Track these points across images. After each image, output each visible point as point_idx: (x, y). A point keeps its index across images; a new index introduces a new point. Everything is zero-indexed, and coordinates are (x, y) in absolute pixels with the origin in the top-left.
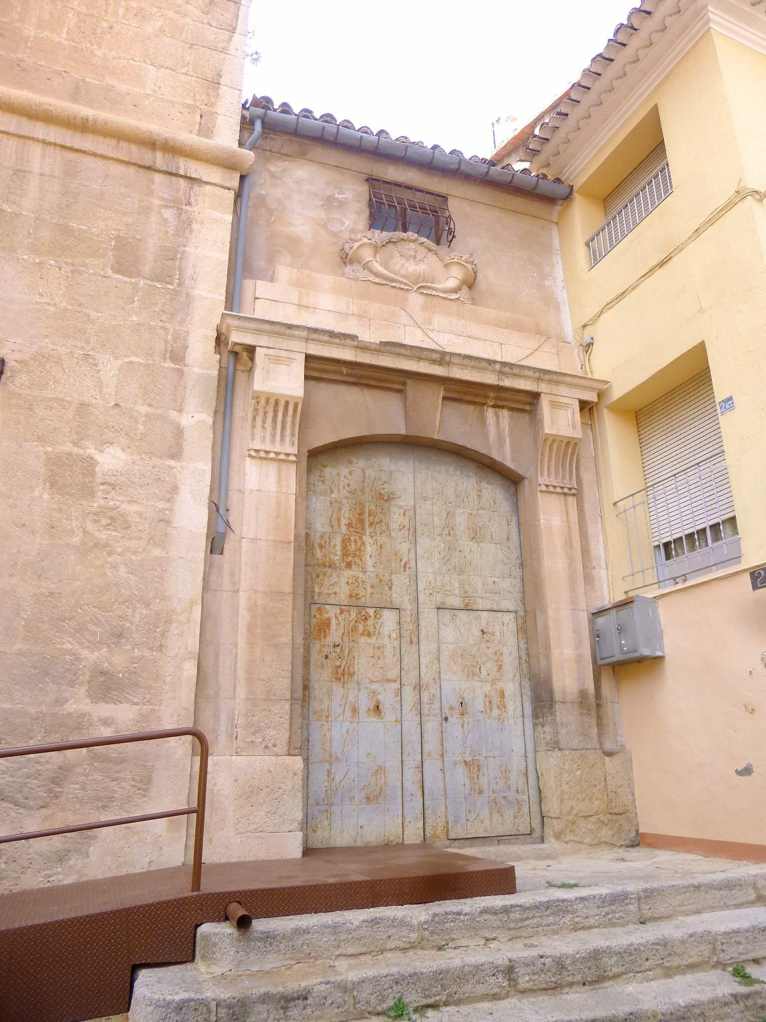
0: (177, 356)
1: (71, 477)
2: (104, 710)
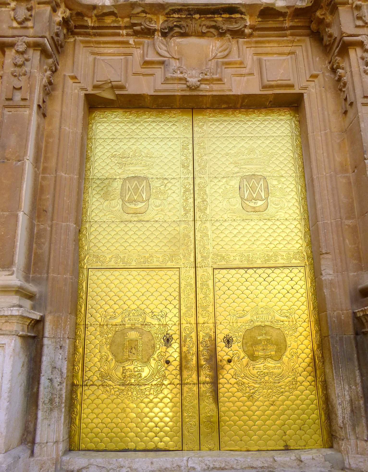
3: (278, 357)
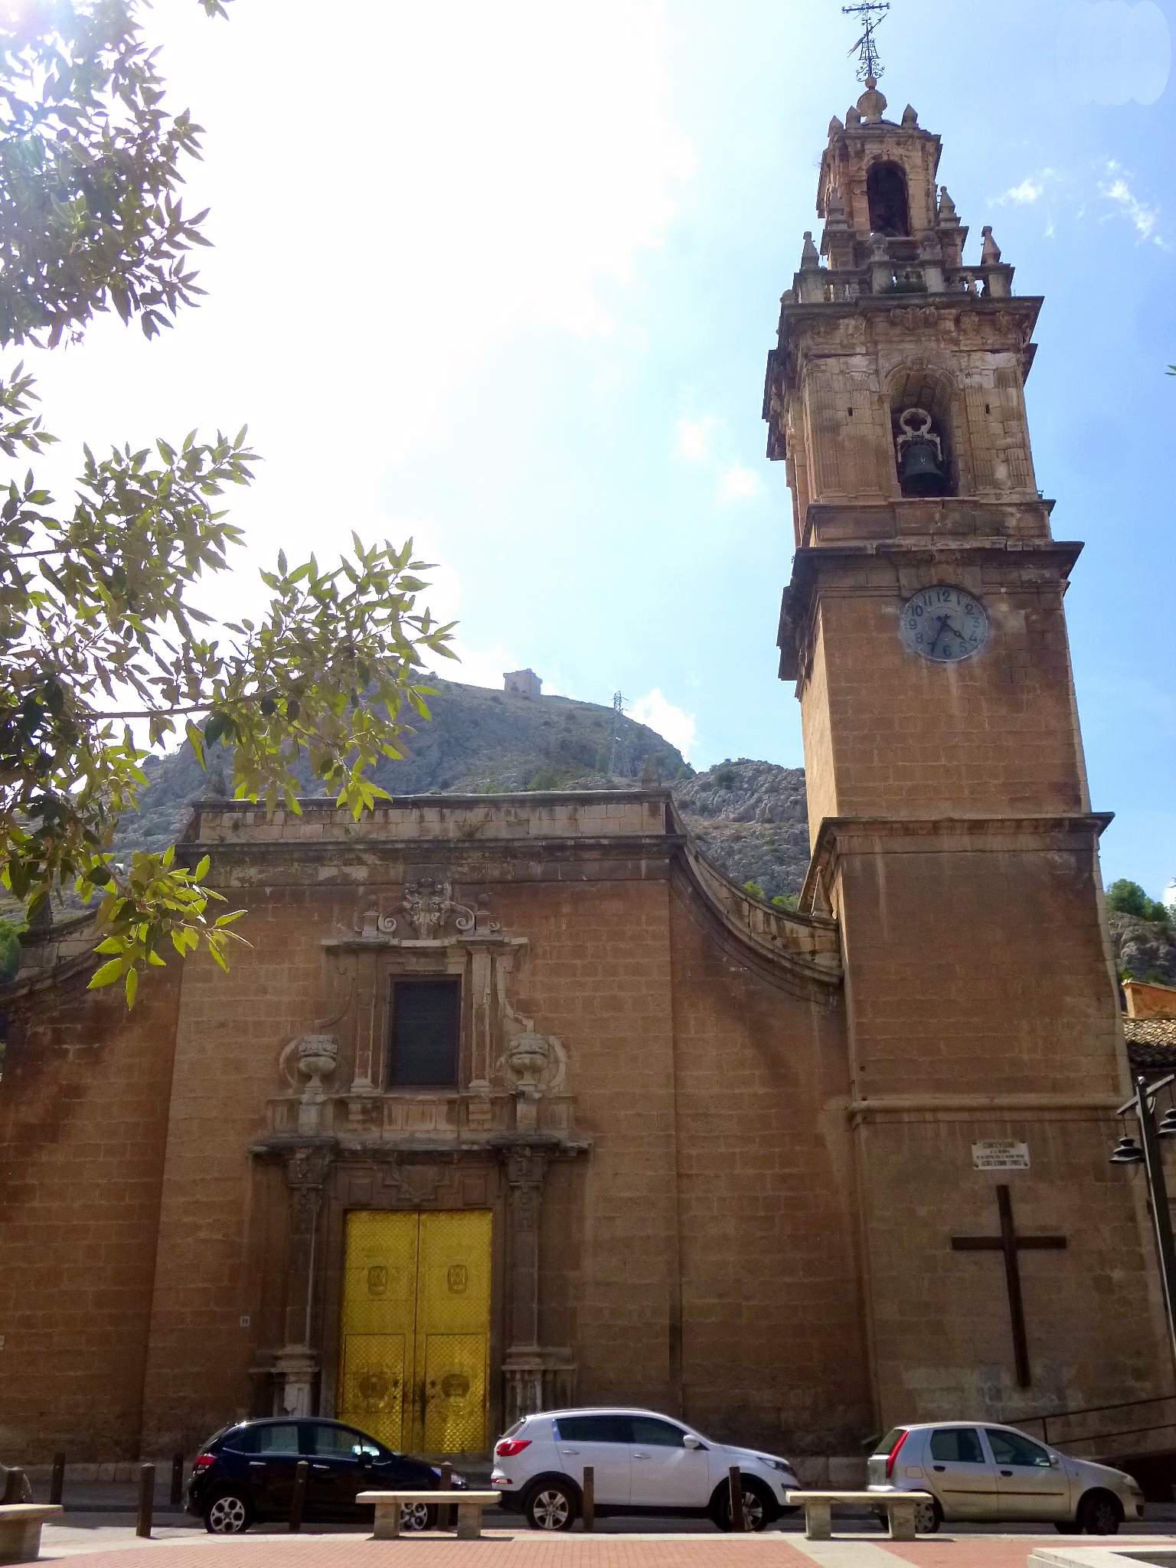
0: (1132, 1218)
1: (1104, 1285)
2: (1138, 1385)
3: (463, 1395)
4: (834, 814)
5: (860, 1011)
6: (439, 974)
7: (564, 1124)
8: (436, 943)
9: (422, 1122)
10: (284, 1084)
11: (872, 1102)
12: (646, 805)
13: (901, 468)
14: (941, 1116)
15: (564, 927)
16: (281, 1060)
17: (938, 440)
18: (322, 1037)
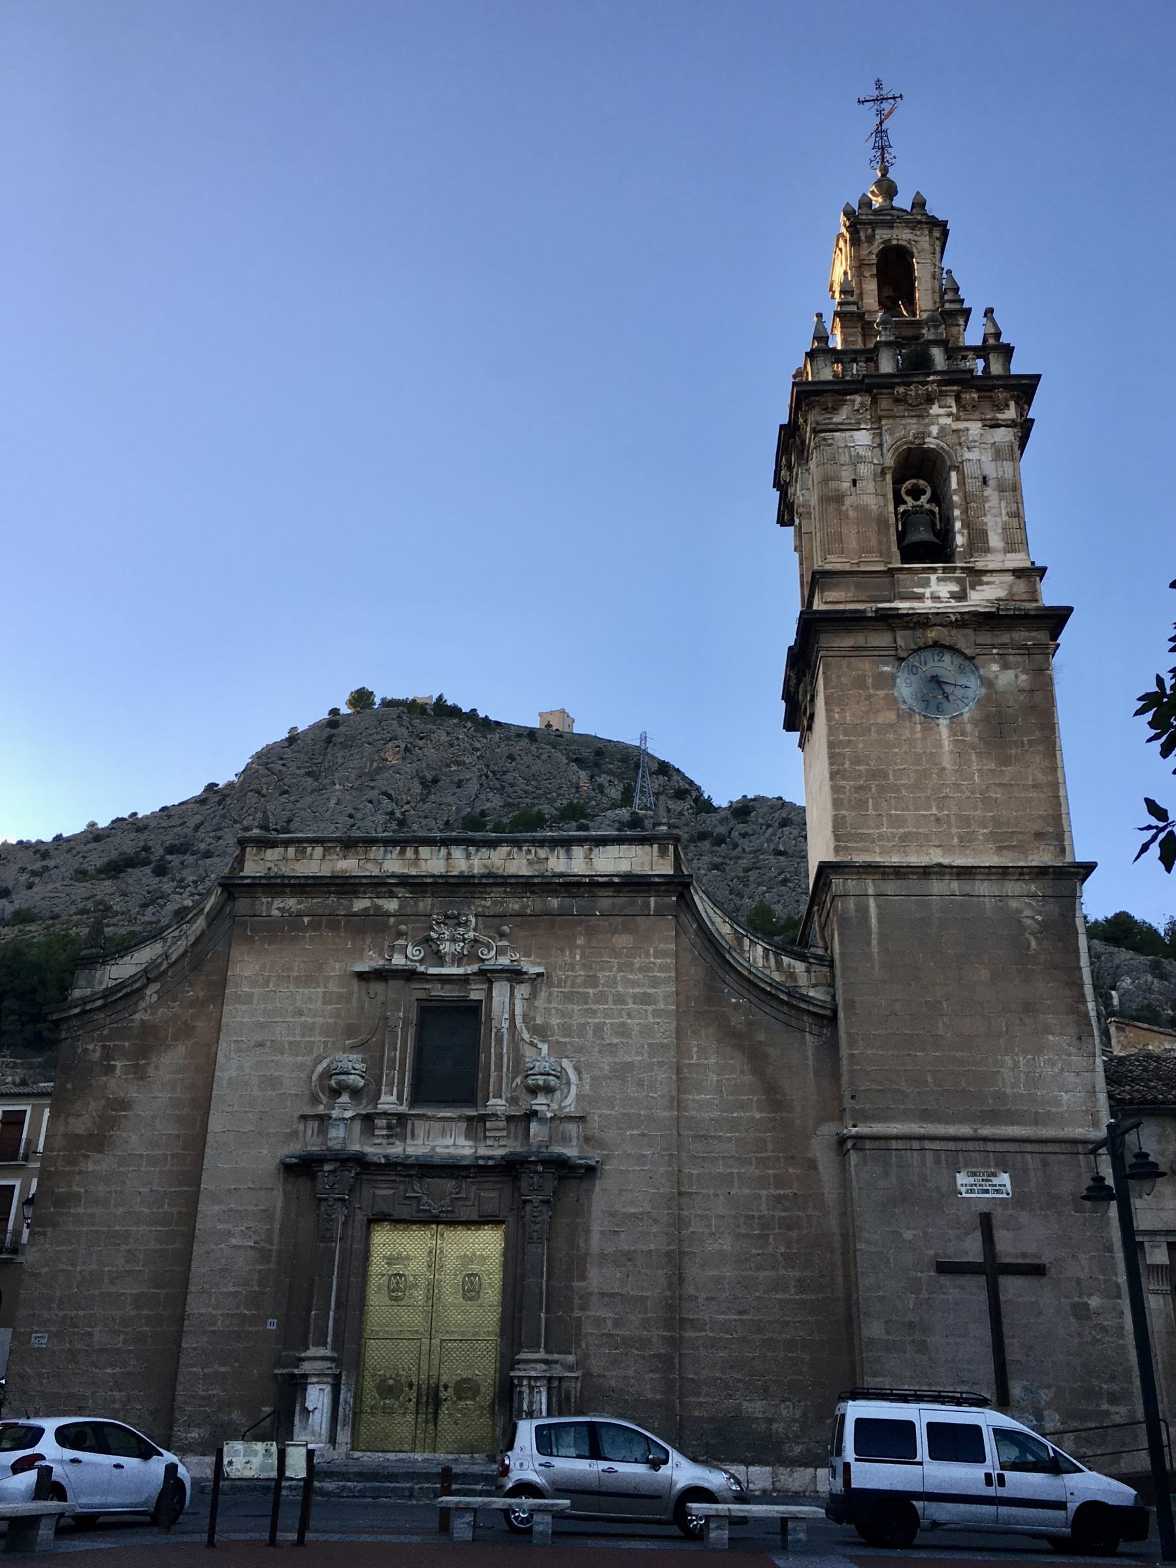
1: (1081, 1312)
4: (830, 857)
5: (852, 1044)
6: (464, 999)
7: (574, 1143)
8: (460, 971)
9: (444, 1139)
10: (315, 1100)
11: (862, 1129)
12: (656, 846)
13: (901, 536)
14: (927, 1144)
15: (578, 958)
16: (314, 1078)
17: (937, 510)
18: (353, 1057)
